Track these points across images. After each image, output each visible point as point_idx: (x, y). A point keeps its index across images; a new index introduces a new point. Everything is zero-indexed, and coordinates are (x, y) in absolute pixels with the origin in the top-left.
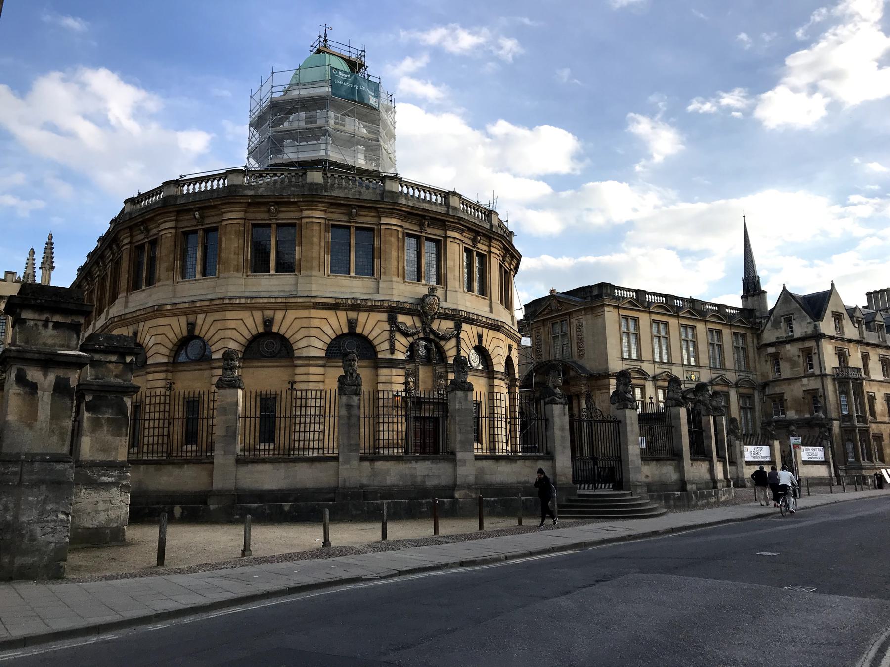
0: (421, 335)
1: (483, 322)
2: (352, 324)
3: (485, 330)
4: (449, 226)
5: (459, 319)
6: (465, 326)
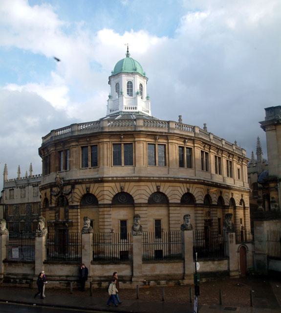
0: (60, 195)
1: (86, 182)
2: (46, 194)
3: (92, 185)
4: (69, 142)
5: (74, 183)
6: (77, 186)
